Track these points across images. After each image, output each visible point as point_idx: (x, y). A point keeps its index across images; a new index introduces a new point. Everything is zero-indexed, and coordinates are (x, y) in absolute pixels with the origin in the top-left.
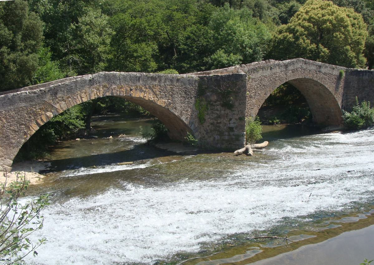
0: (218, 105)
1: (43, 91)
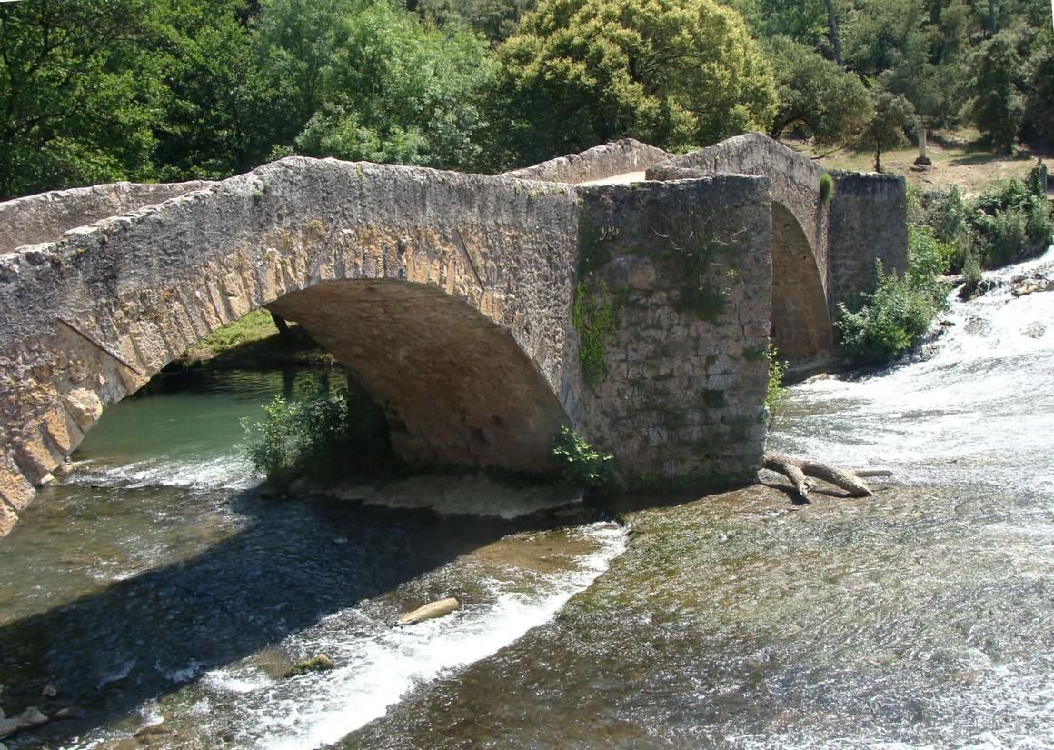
0: (659, 306)
1: (49, 265)
